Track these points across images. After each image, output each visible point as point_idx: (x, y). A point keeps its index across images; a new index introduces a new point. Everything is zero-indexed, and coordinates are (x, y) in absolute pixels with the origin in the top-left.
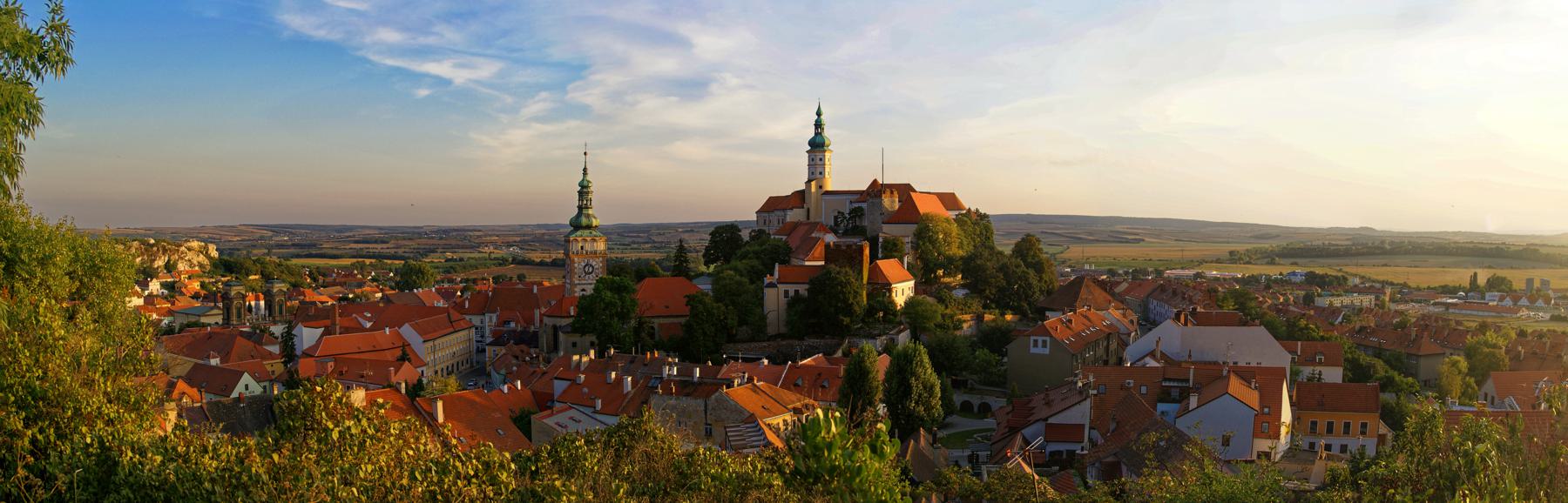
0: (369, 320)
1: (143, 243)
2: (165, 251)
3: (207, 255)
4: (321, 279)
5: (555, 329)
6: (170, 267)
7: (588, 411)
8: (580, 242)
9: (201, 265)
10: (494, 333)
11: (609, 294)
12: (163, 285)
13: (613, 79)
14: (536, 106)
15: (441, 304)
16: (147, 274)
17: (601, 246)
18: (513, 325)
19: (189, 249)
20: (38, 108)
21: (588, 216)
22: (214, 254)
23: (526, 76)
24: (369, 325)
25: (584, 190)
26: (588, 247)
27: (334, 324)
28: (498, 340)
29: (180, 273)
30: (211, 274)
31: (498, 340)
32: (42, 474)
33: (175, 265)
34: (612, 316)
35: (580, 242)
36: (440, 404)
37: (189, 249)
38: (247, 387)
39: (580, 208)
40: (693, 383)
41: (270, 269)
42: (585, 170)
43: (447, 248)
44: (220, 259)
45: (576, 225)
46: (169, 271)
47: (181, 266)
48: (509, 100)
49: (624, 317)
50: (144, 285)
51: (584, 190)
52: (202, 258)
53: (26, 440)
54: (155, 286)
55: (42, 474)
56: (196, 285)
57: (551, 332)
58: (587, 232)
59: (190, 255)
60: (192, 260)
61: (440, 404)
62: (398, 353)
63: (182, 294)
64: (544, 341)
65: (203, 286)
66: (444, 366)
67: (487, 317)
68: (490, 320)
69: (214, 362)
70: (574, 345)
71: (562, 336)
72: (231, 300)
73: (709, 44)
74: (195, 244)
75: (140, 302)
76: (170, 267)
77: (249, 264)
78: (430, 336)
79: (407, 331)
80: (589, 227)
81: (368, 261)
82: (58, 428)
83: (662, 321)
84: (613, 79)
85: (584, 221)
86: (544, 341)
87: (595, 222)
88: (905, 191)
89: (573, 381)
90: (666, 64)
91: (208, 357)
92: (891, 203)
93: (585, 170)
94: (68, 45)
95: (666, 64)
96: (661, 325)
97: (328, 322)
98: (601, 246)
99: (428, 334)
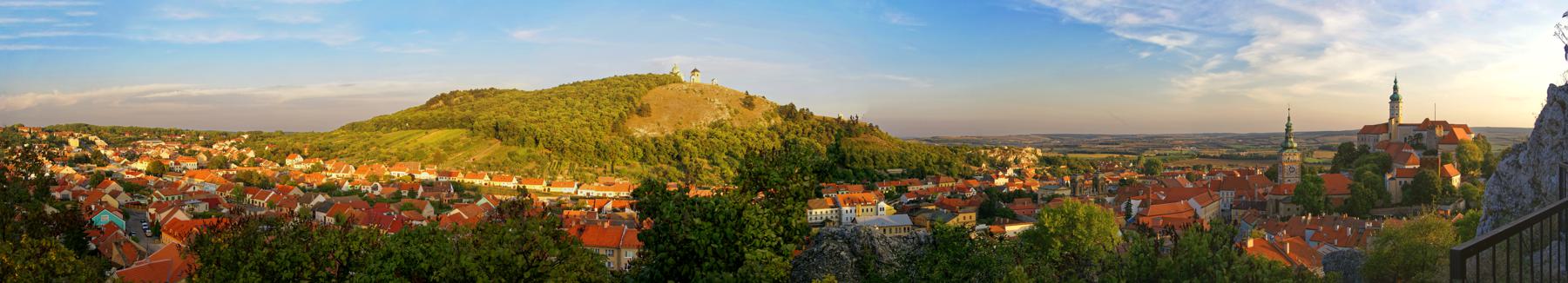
5: (1277, 202)
13: (1269, 45)
14: (1213, 63)
15: (1190, 185)
16: (1004, 166)
23: (1212, 44)
25: (1288, 127)
28: (1238, 205)
43: (1159, 147)
48: (1198, 58)
51: (1288, 127)
64: (1271, 207)
68: (1228, 196)
73: (1332, 22)
84: (1269, 45)
86: (1271, 207)
88: (1444, 124)
90: (1303, 35)
92: (1440, 132)
95: (1303, 35)
98: (1297, 158)
99: (1203, 204)
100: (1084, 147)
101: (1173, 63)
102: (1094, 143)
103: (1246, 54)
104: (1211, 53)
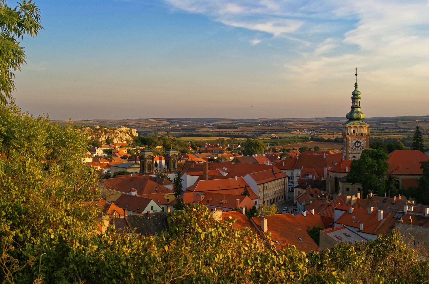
0: (226, 172)
1: (92, 128)
2: (106, 133)
3: (131, 135)
4: (198, 150)
5: (336, 179)
6: (108, 142)
7: (355, 230)
8: (353, 128)
9: (127, 140)
10: (299, 181)
11: (370, 159)
12: (105, 151)
15: (268, 163)
16: (95, 145)
17: (366, 130)
18: (310, 176)
19: (121, 132)
20: (21, 53)
21: (358, 112)
22: (135, 134)
23: (317, 29)
24: (225, 175)
25: (355, 97)
26: (358, 131)
27: (205, 174)
28: (302, 185)
29: (115, 145)
30: (133, 145)
31: (302, 185)
32: (19, 256)
33: (112, 141)
34: (372, 173)
35: (353, 128)
36: (265, 221)
37: (121, 132)
38: (152, 208)
39: (353, 108)
40: (424, 218)
41: (169, 143)
42: (356, 85)
43: (272, 131)
44: (139, 137)
45: (350, 118)
46: (108, 143)
47: (116, 141)
48: (308, 44)
49: (379, 174)
50: (93, 151)
51: (355, 97)
52: (128, 136)
53: (11, 238)
54: (99, 152)
55: (19, 256)
56: (124, 151)
57: (334, 181)
58: (357, 122)
59: (121, 135)
60: (122, 138)
61: (265, 221)
62: (242, 191)
63: (116, 156)
64: (329, 186)
65: (128, 151)
66: (269, 199)
67: (295, 171)
68: (297, 173)
69: (134, 193)
70: (348, 189)
71: (340, 184)
72: (145, 160)
74: (124, 129)
75: (91, 160)
76: (108, 142)
77: (156, 140)
78: (260, 182)
79: (248, 178)
80: (358, 119)
81: (226, 139)
82: (33, 230)
83: (404, 177)
85: (355, 115)
86: (329, 186)
87: (362, 116)
89: (347, 211)
91: (130, 191)
93: (356, 85)
94: (37, 17)
96: (403, 180)
97: (202, 173)
98: (366, 130)
99: (260, 181)
100: (202, 130)
101: (282, 46)
102: (214, 127)
103: (351, 38)
104: (320, 38)
